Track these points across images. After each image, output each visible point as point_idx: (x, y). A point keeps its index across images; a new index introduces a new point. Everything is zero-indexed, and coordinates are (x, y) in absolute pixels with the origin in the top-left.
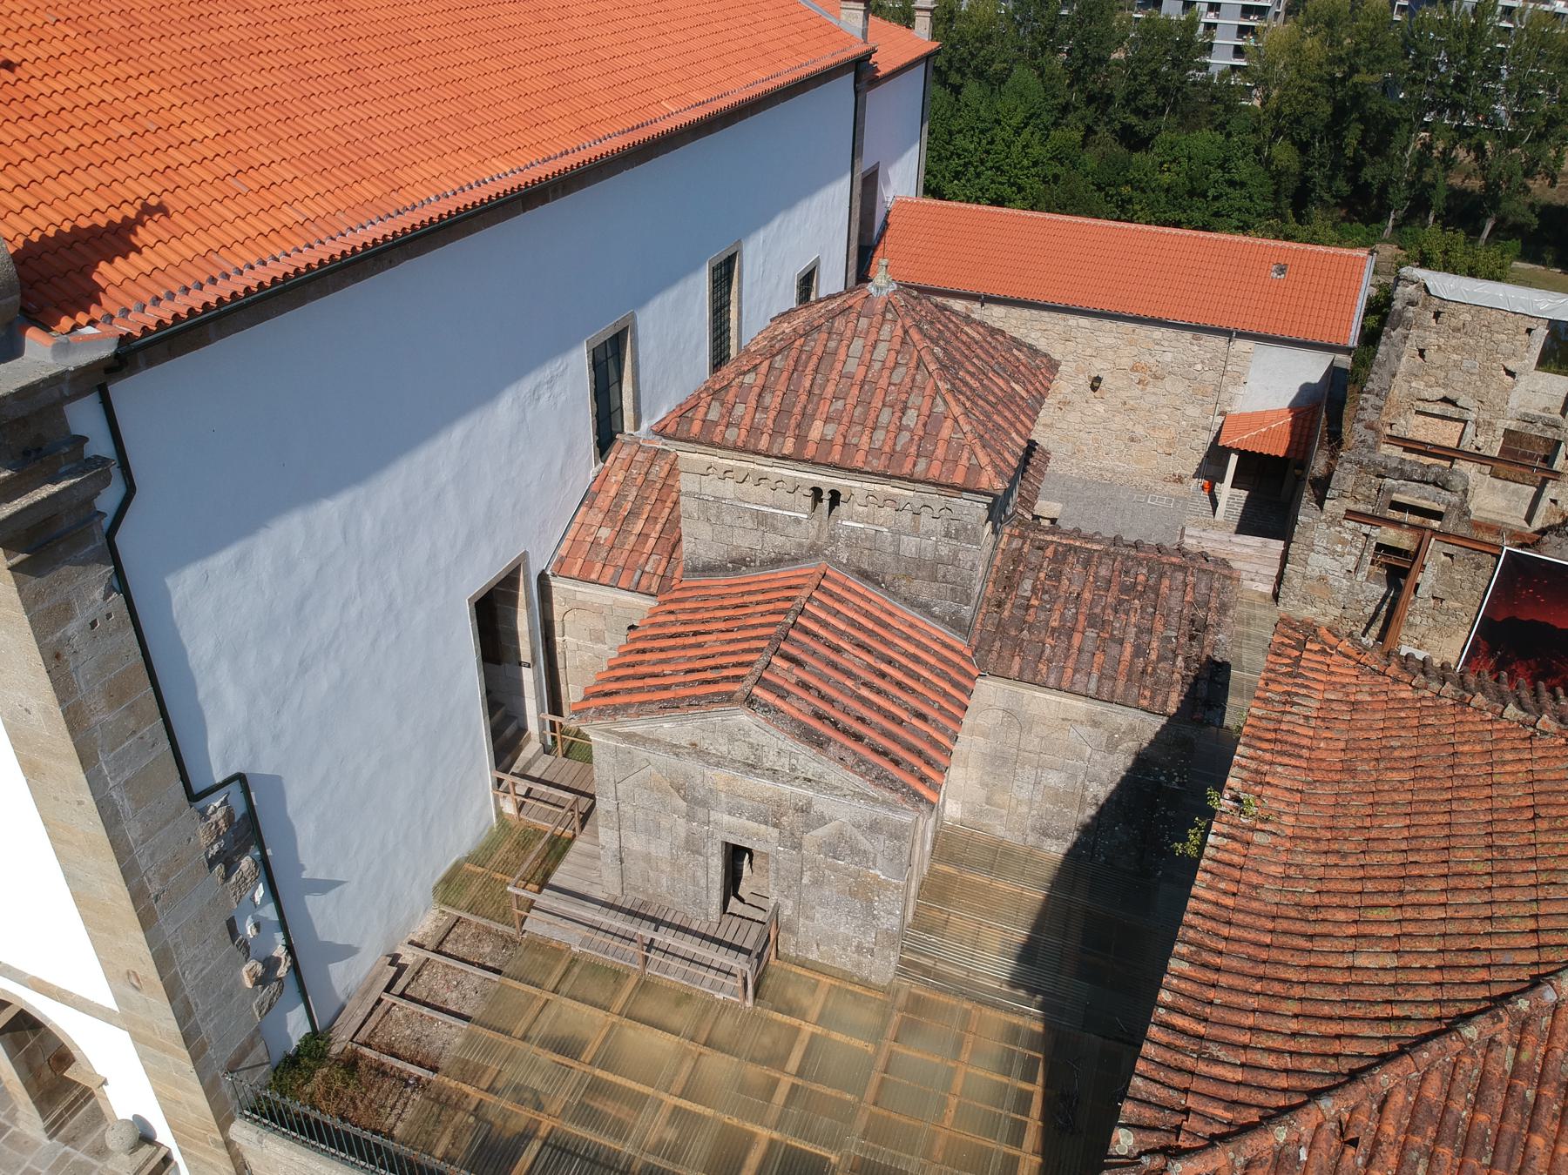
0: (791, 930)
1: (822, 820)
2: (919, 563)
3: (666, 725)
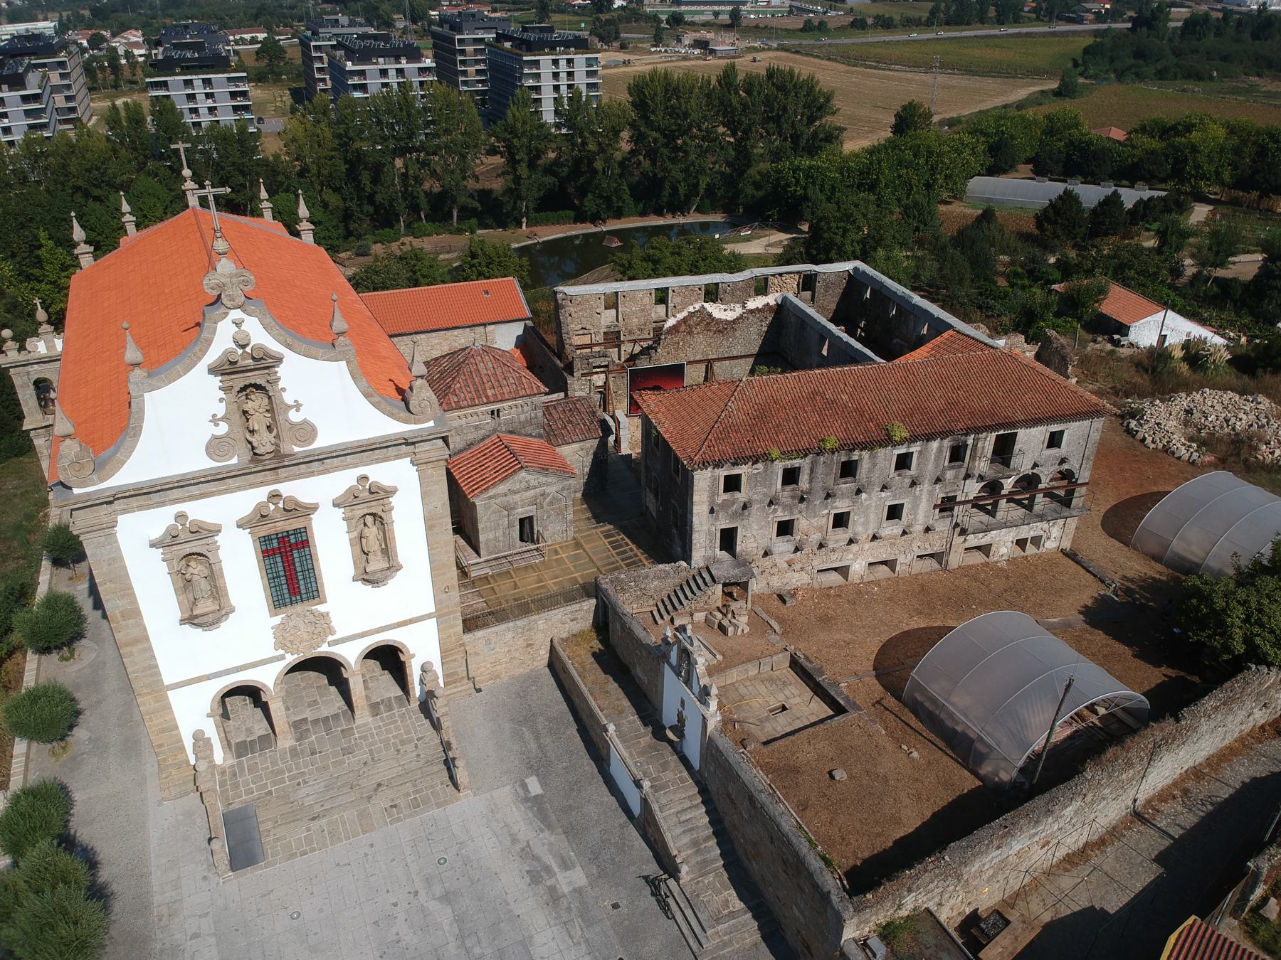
1: (549, 494)
2: (526, 421)
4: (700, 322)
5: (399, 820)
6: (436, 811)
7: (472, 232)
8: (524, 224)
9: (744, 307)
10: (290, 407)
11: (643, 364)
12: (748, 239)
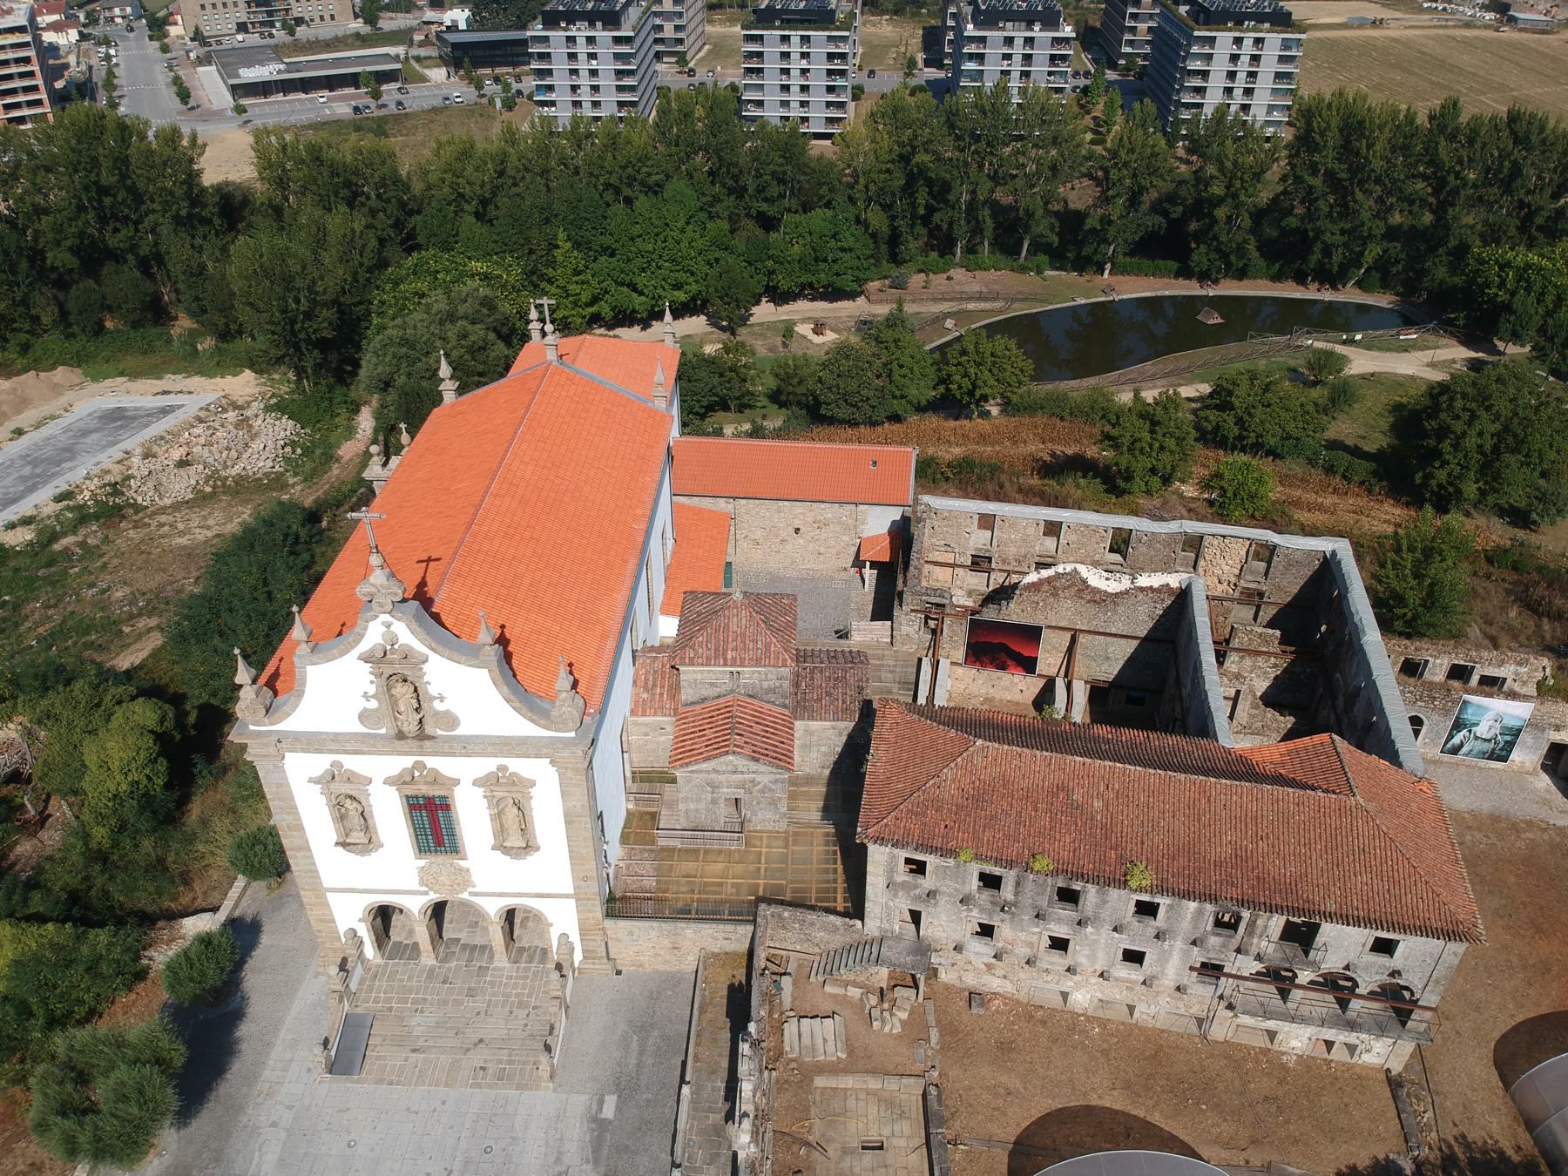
0: (750, 821)
4: (1069, 587)
5: (479, 1086)
6: (514, 1092)
7: (1039, 272)
8: (1107, 272)
9: (1132, 583)
10: (435, 698)
11: (990, 614)
12: (1406, 348)
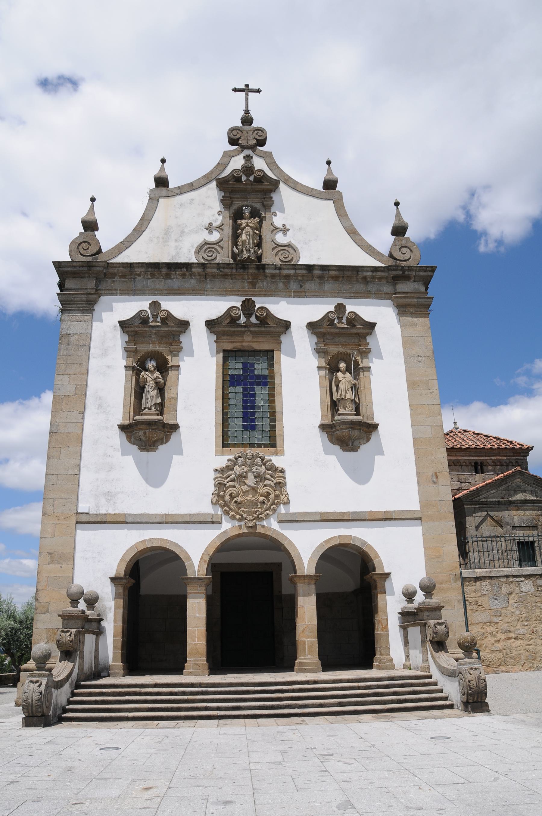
3: (492, 492)
